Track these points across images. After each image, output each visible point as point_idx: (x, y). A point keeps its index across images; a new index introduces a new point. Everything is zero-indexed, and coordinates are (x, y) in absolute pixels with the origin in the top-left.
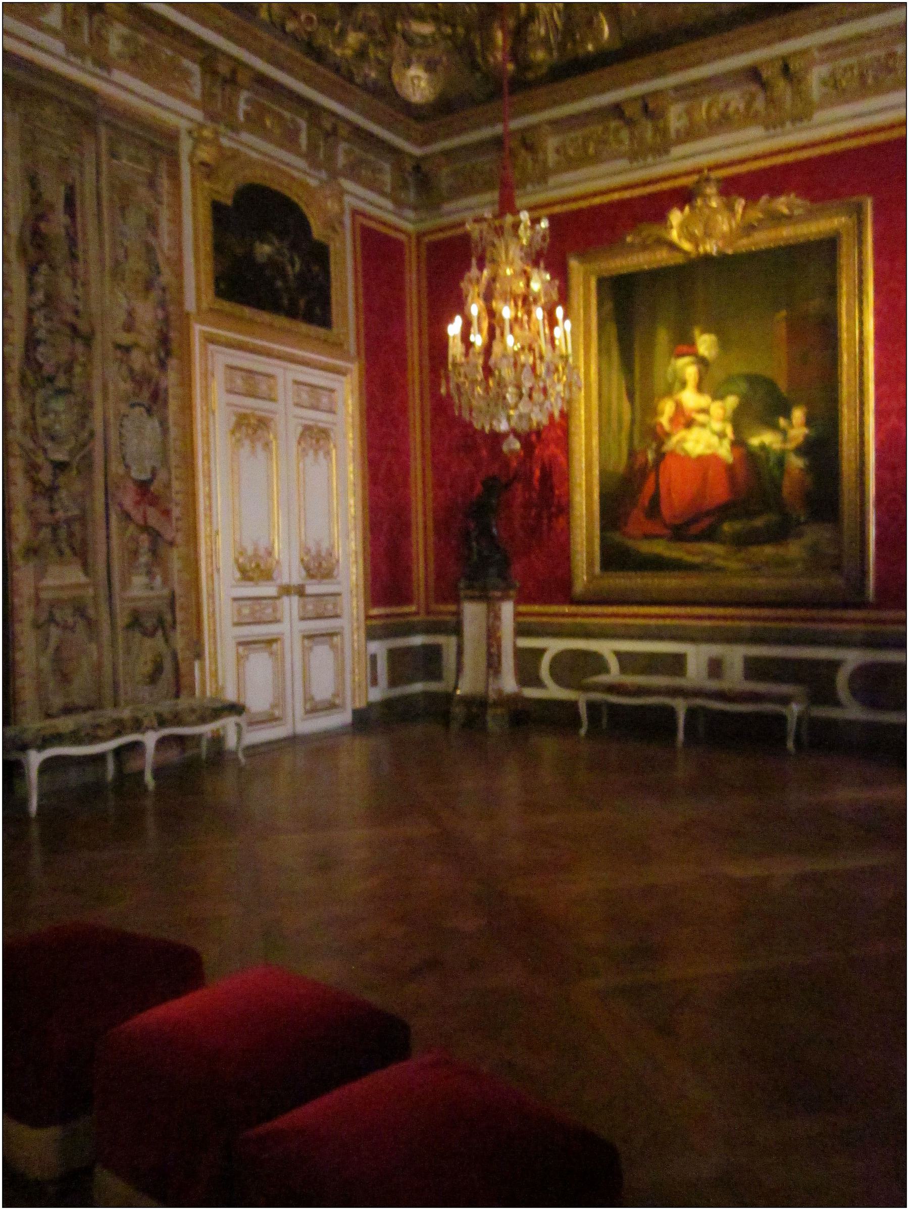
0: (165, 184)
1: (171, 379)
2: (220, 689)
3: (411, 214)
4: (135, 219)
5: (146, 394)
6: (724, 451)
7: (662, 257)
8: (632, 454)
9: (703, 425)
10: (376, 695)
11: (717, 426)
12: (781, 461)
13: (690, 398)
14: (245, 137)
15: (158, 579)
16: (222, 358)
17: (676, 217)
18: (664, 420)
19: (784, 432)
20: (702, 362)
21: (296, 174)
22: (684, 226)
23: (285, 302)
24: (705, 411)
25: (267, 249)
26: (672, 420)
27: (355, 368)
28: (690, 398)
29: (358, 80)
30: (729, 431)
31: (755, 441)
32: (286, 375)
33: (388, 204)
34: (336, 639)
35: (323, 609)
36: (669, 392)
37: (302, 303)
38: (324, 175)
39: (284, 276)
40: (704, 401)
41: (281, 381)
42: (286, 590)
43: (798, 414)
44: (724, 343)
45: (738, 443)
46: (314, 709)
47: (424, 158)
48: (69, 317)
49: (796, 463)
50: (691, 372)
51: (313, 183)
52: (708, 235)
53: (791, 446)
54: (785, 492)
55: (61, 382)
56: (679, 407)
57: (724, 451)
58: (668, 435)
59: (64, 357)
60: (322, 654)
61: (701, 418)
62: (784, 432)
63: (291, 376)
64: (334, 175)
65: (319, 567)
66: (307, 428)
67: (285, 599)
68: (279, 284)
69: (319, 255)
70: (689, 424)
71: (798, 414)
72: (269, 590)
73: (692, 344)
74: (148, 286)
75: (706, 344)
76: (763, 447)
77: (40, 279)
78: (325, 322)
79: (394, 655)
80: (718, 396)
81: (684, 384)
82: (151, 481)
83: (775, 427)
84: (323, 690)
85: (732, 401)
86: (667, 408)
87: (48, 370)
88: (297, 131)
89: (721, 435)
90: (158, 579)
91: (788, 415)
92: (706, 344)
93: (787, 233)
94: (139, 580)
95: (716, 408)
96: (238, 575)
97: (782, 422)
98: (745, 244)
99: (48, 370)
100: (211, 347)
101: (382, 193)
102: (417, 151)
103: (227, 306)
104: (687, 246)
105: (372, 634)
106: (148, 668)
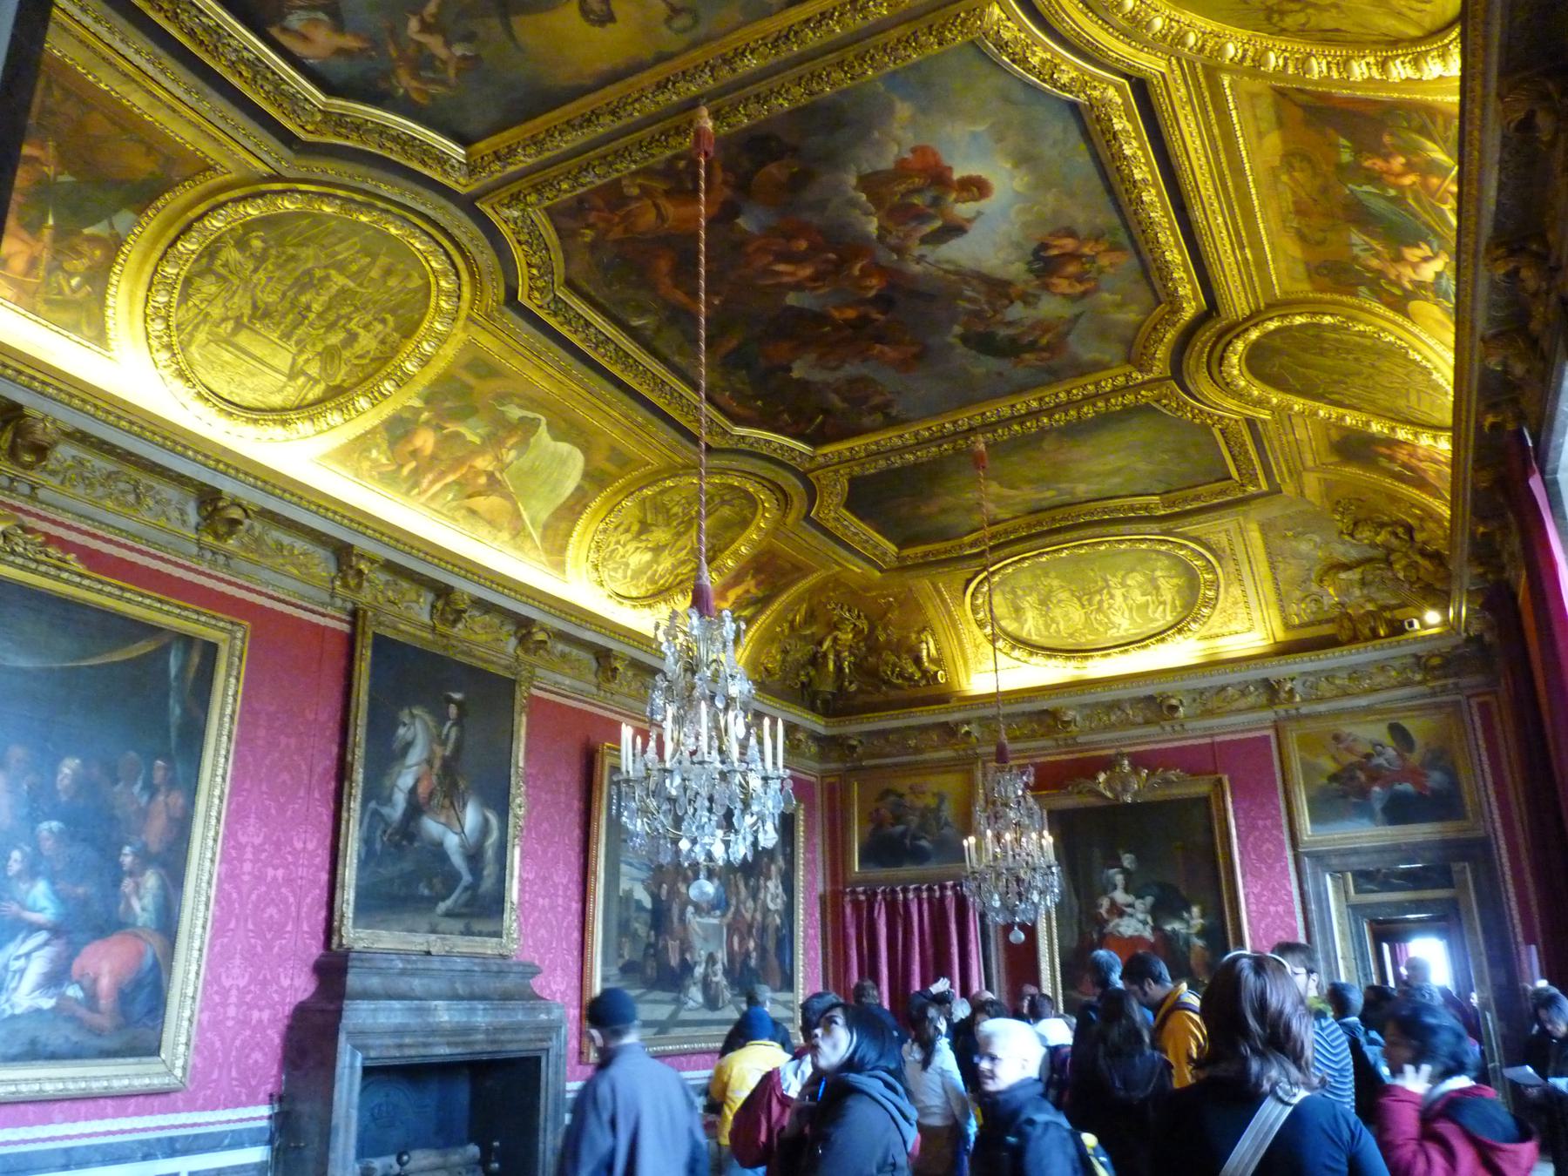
6: (1147, 933)
7: (1091, 801)
8: (1081, 934)
9: (1131, 916)
11: (1141, 916)
12: (1187, 943)
13: (1120, 896)
17: (1102, 777)
18: (1103, 911)
19: (1188, 922)
20: (1125, 871)
22: (1108, 781)
24: (1131, 906)
26: (1109, 911)
28: (1120, 896)
30: (1149, 920)
31: (1168, 928)
36: (1105, 892)
40: (1130, 899)
43: (1195, 910)
44: (1140, 859)
45: (1157, 929)
49: (1199, 943)
50: (1119, 879)
52: (1125, 790)
53: (1193, 931)
54: (1193, 962)
56: (1113, 903)
57: (1147, 933)
58: (1107, 922)
61: (1129, 910)
62: (1188, 922)
70: (1121, 914)
71: (1195, 910)
73: (1119, 859)
75: (1128, 860)
76: (1174, 931)
80: (1139, 896)
81: (1115, 887)
83: (1181, 919)
85: (1149, 900)
86: (1105, 903)
89: (1145, 923)
91: (1189, 912)
92: (1128, 860)
93: (1177, 792)
95: (1139, 904)
97: (1186, 915)
98: (1149, 797)
104: (1109, 794)
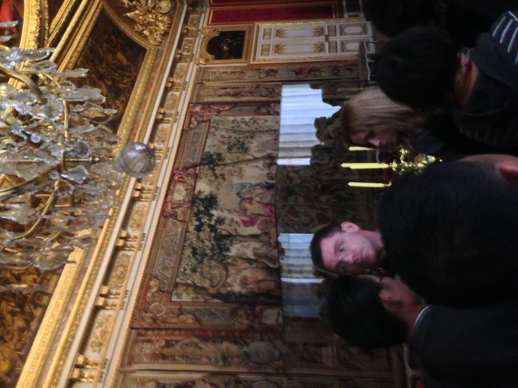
0: (213, 70)
1: (266, 68)
2: (356, 55)
3: (204, 9)
4: (225, 76)
5: (272, 73)
10: (362, 15)
14: (194, 52)
15: (324, 70)
16: (259, 56)
21: (201, 40)
23: (239, 42)
25: (225, 47)
27: (256, 24)
29: (169, 22)
32: (261, 41)
33: (203, 15)
34: (343, 26)
35: (333, 31)
37: (239, 38)
38: (199, 33)
39: (231, 43)
41: (264, 43)
42: (327, 40)
46: (365, 31)
47: (188, 4)
48: (254, 88)
51: (202, 36)
55: (271, 90)
59: (264, 90)
60: (347, 30)
63: (262, 40)
64: (198, 30)
65: (320, 32)
66: (277, 36)
67: (330, 40)
68: (234, 44)
69: (223, 35)
72: (327, 45)
74: (242, 73)
77: (245, 94)
78: (243, 32)
79: (349, 10)
82: (295, 71)
84: (359, 29)
87: (268, 93)
88: (188, 40)
90: (324, 70)
94: (323, 74)
96: (322, 52)
99: (268, 93)
100: (256, 60)
101: (200, 17)
102: (186, 6)
103: (244, 56)
105: (342, 17)
106: (349, 71)
